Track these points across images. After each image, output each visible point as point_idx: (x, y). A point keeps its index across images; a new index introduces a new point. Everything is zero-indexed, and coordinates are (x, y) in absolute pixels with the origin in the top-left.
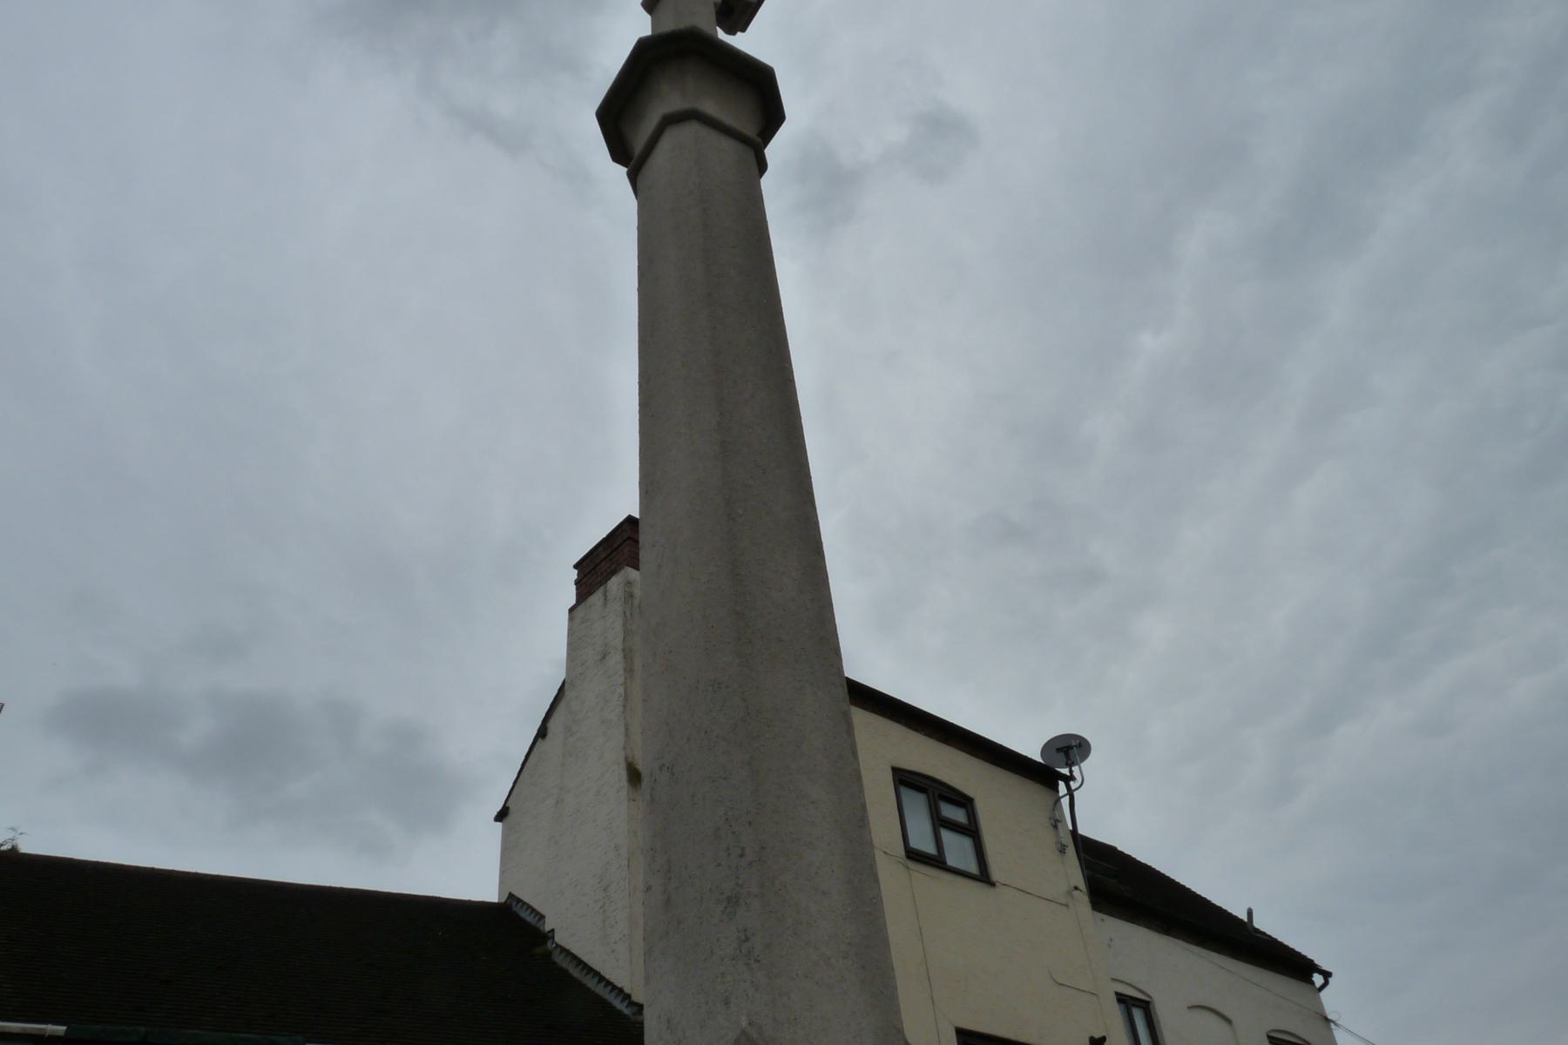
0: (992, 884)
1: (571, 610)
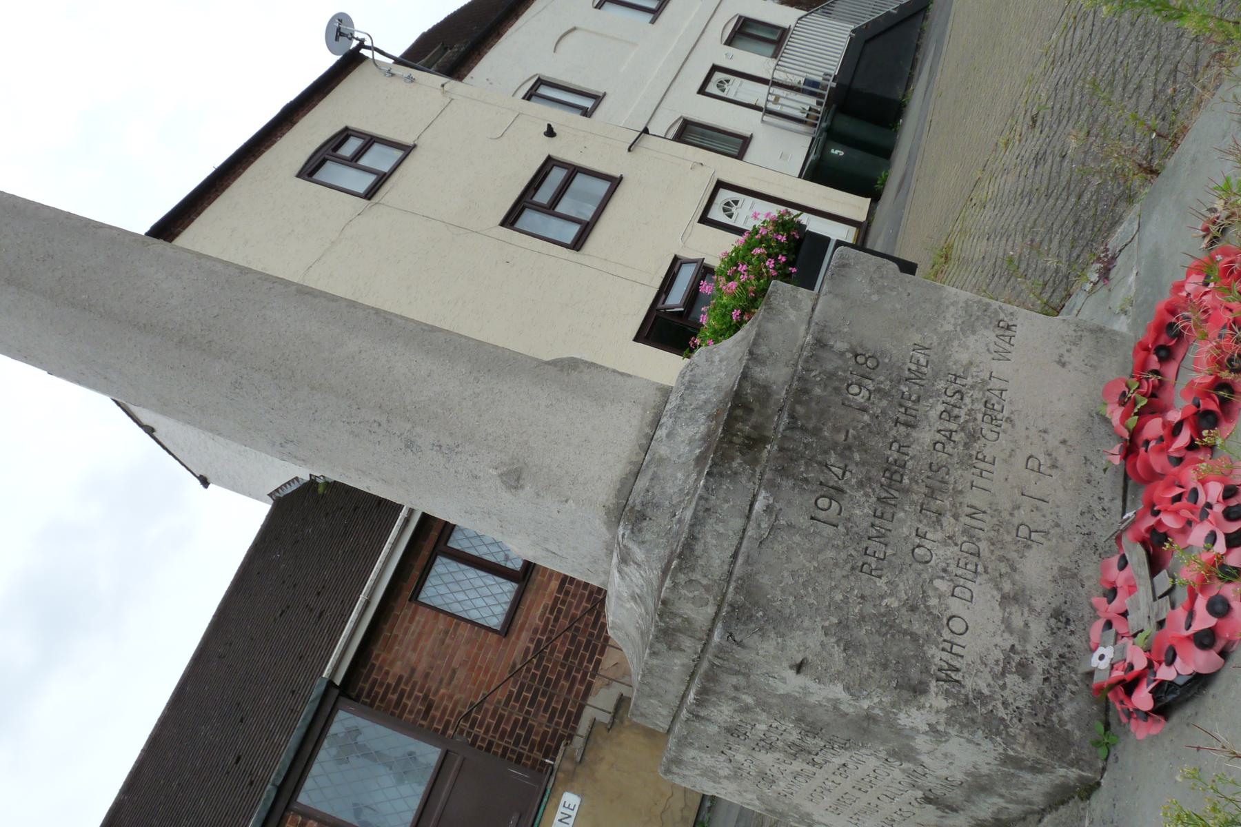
0: (415, 146)
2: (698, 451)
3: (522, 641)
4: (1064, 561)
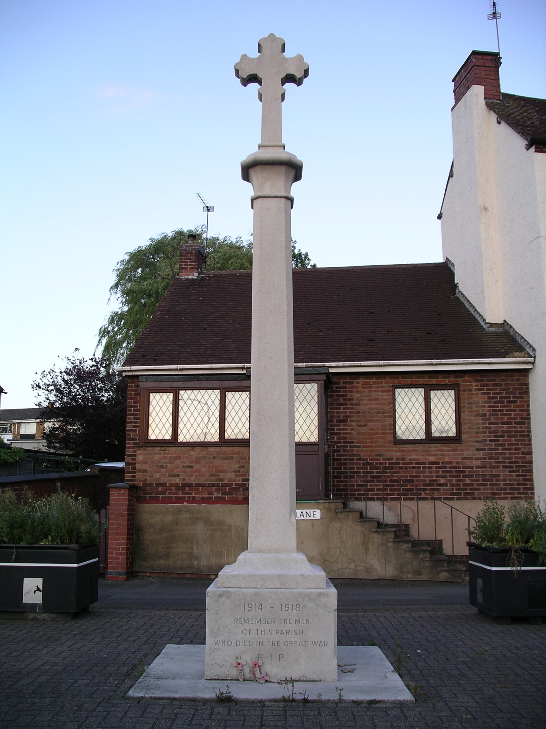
1: (452, 109)
3: (395, 453)
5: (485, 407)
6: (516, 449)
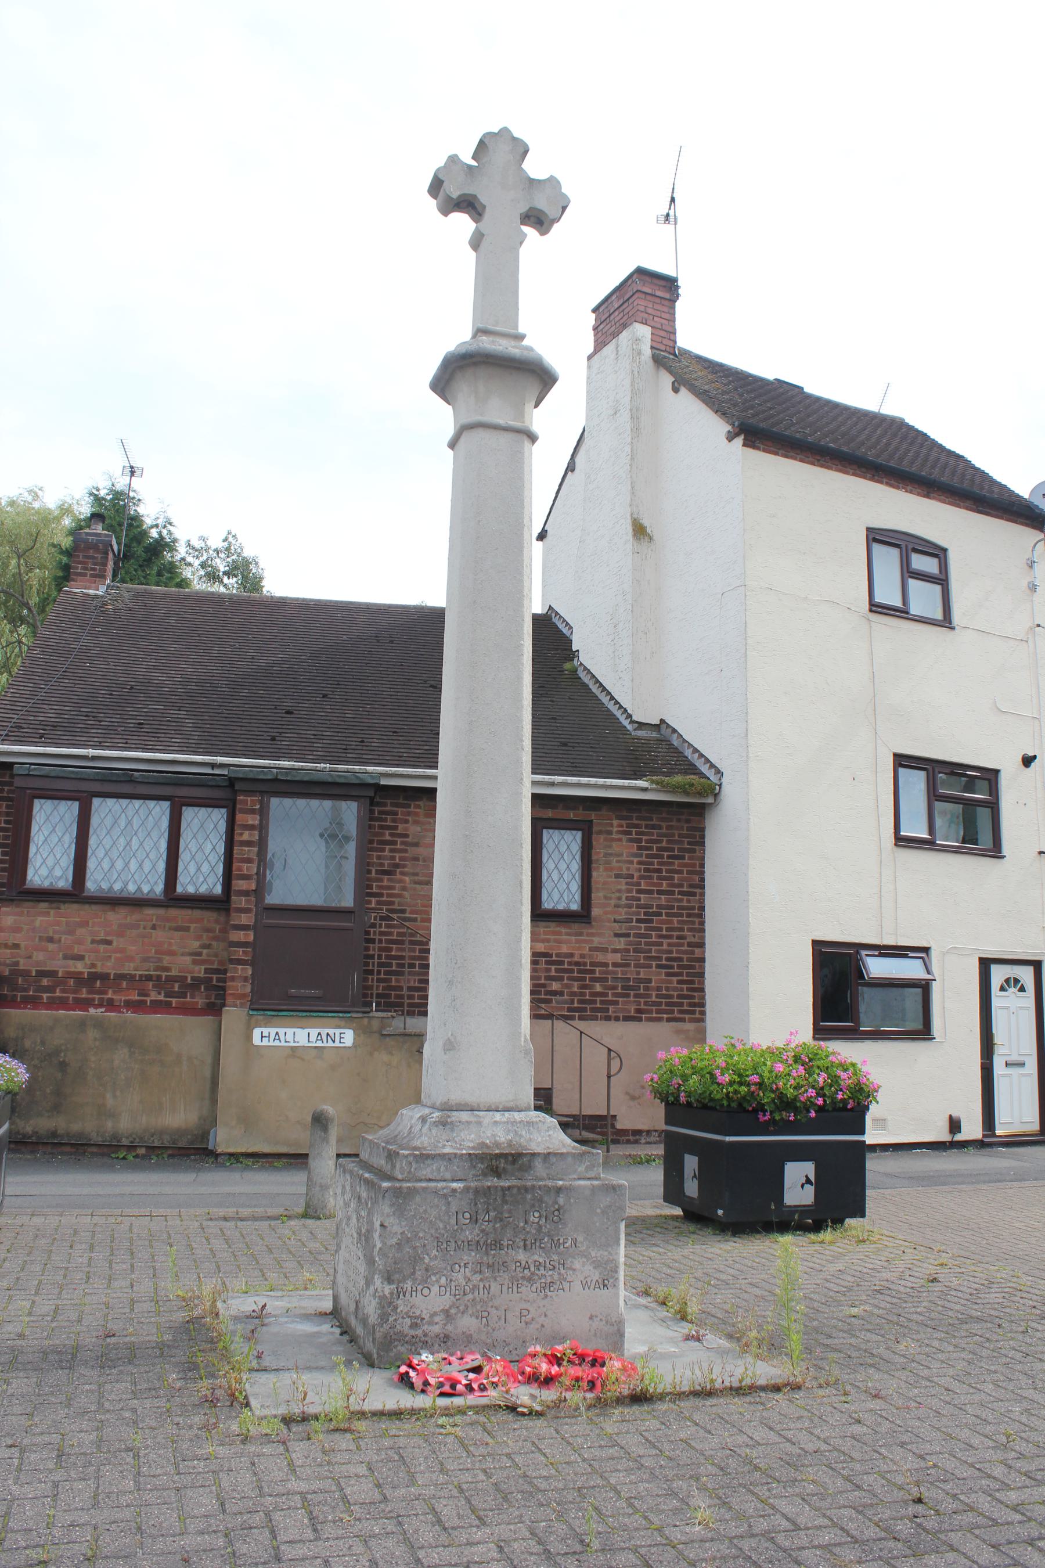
0: (953, 628)
1: (589, 358)
2: (488, 1142)
4: (475, 1336)
5: (632, 862)
6: (679, 937)
